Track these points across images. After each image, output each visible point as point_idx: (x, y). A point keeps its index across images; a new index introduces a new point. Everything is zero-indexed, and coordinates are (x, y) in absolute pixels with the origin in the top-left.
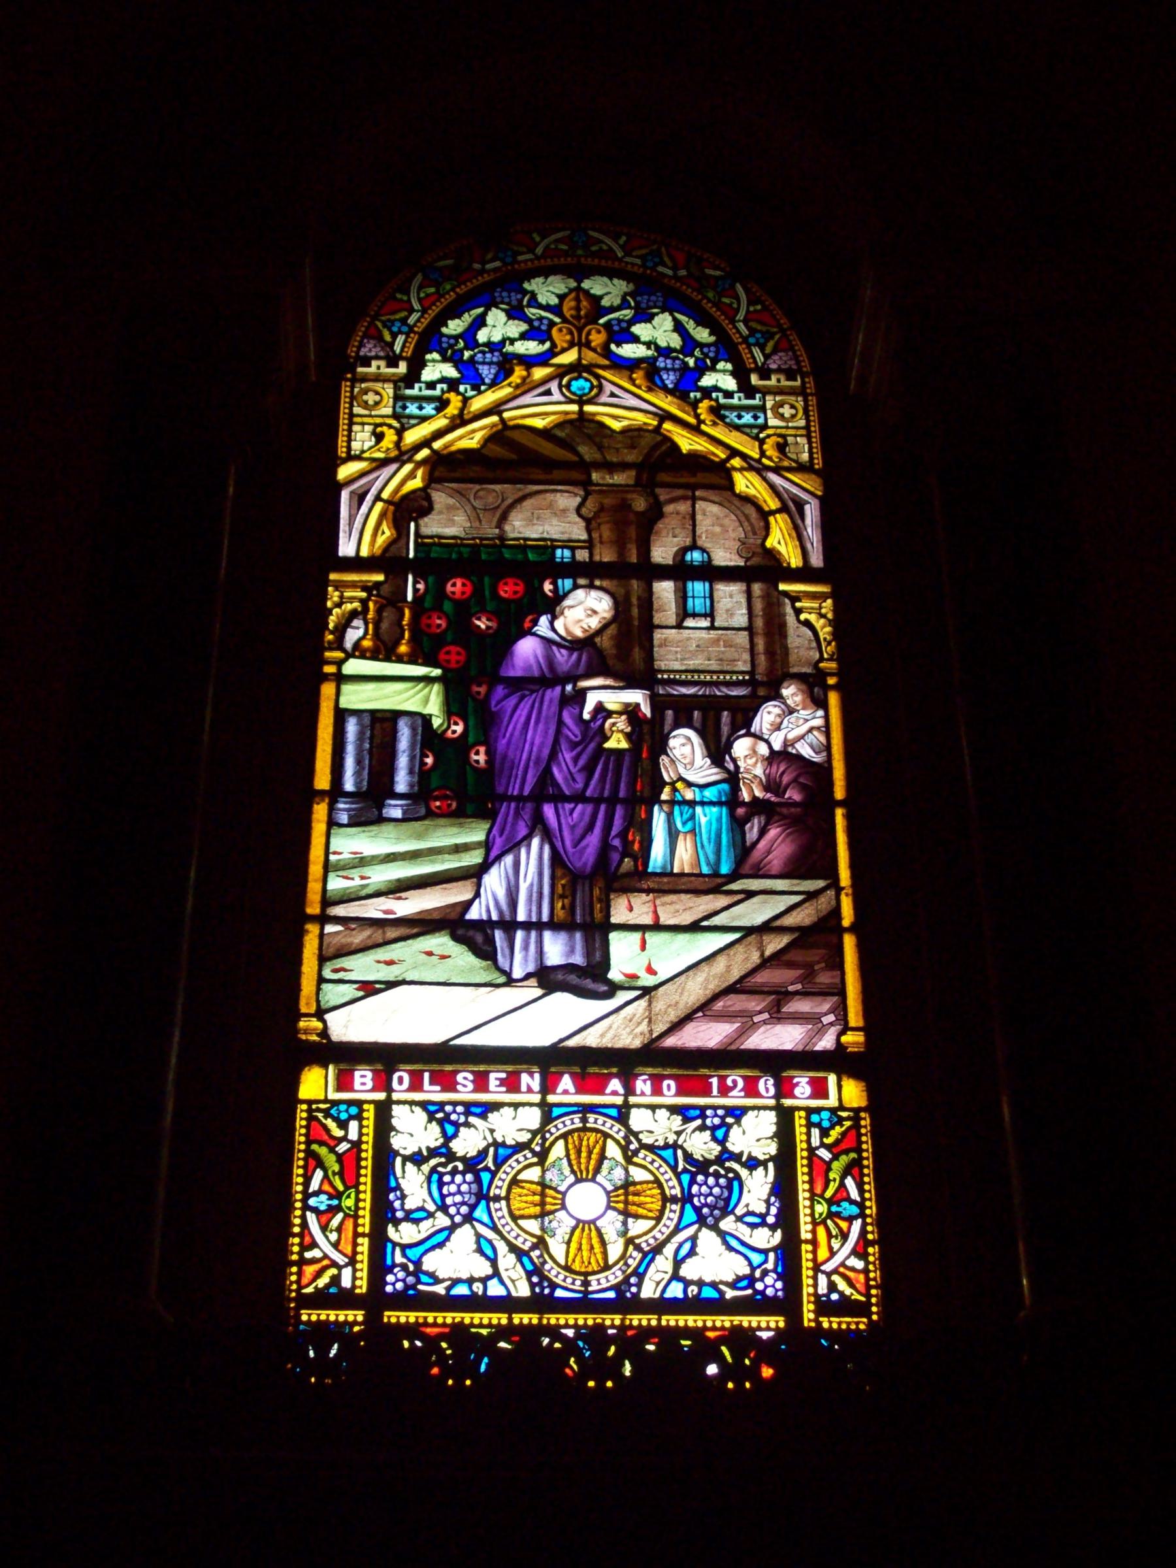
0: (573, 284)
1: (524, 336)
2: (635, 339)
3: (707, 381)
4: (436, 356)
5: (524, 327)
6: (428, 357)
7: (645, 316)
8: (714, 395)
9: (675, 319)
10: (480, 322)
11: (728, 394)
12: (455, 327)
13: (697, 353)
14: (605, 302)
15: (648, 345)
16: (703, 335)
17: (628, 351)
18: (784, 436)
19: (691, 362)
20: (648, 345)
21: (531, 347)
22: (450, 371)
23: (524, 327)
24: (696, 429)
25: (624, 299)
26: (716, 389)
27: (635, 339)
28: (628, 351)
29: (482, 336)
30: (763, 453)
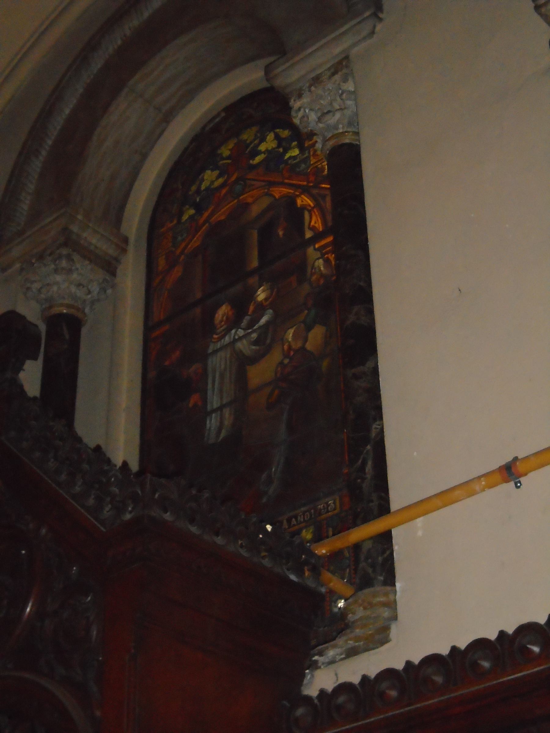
0: (235, 141)
1: (218, 177)
2: (259, 153)
3: (287, 156)
4: (187, 207)
5: (217, 172)
6: (184, 209)
7: (263, 139)
8: (290, 162)
9: (274, 132)
10: (203, 180)
11: (294, 158)
12: (194, 188)
13: (284, 144)
14: (248, 142)
15: (264, 153)
16: (285, 133)
17: (258, 159)
18: (316, 167)
19: (281, 150)
20: (264, 153)
21: (221, 180)
22: (192, 212)
23: (217, 172)
24: (283, 184)
25: (256, 135)
26: (290, 158)
27: (260, 152)
28: (258, 159)
29: (203, 187)
30: (309, 182)
